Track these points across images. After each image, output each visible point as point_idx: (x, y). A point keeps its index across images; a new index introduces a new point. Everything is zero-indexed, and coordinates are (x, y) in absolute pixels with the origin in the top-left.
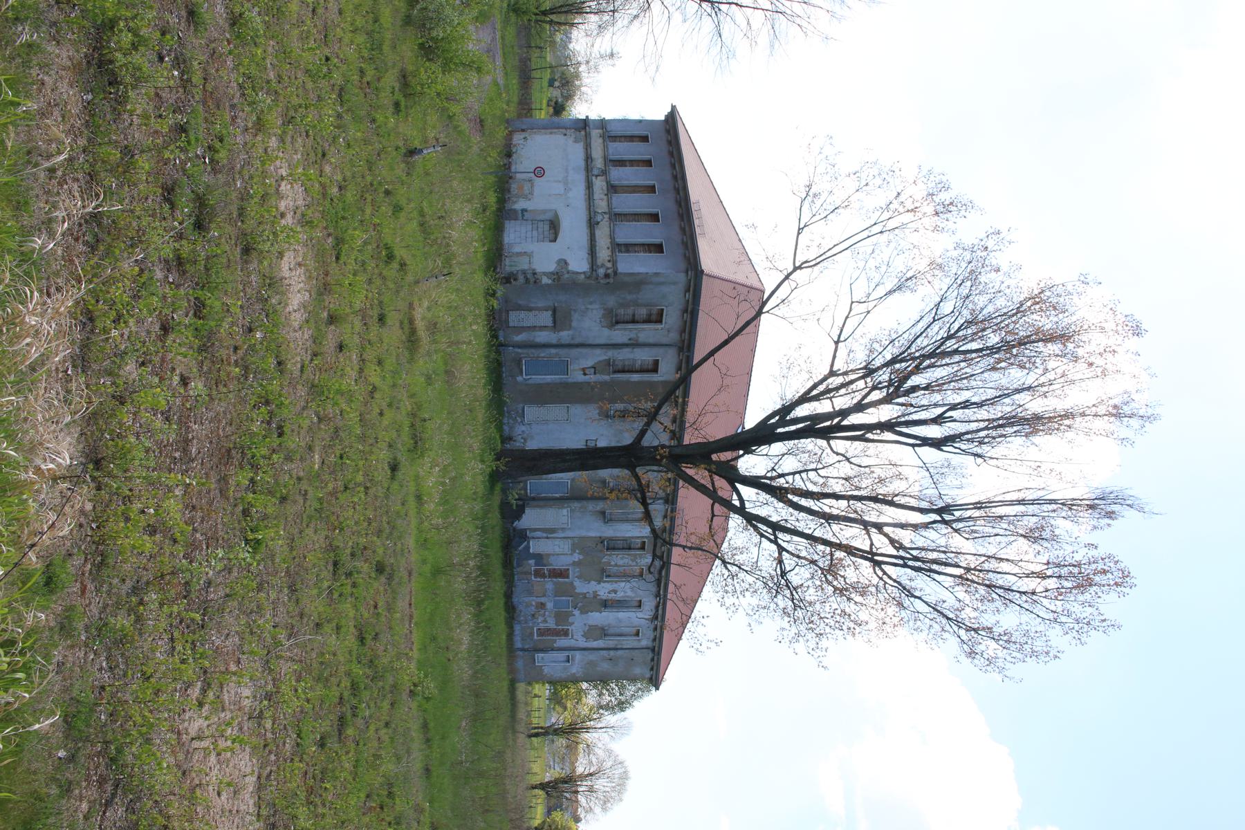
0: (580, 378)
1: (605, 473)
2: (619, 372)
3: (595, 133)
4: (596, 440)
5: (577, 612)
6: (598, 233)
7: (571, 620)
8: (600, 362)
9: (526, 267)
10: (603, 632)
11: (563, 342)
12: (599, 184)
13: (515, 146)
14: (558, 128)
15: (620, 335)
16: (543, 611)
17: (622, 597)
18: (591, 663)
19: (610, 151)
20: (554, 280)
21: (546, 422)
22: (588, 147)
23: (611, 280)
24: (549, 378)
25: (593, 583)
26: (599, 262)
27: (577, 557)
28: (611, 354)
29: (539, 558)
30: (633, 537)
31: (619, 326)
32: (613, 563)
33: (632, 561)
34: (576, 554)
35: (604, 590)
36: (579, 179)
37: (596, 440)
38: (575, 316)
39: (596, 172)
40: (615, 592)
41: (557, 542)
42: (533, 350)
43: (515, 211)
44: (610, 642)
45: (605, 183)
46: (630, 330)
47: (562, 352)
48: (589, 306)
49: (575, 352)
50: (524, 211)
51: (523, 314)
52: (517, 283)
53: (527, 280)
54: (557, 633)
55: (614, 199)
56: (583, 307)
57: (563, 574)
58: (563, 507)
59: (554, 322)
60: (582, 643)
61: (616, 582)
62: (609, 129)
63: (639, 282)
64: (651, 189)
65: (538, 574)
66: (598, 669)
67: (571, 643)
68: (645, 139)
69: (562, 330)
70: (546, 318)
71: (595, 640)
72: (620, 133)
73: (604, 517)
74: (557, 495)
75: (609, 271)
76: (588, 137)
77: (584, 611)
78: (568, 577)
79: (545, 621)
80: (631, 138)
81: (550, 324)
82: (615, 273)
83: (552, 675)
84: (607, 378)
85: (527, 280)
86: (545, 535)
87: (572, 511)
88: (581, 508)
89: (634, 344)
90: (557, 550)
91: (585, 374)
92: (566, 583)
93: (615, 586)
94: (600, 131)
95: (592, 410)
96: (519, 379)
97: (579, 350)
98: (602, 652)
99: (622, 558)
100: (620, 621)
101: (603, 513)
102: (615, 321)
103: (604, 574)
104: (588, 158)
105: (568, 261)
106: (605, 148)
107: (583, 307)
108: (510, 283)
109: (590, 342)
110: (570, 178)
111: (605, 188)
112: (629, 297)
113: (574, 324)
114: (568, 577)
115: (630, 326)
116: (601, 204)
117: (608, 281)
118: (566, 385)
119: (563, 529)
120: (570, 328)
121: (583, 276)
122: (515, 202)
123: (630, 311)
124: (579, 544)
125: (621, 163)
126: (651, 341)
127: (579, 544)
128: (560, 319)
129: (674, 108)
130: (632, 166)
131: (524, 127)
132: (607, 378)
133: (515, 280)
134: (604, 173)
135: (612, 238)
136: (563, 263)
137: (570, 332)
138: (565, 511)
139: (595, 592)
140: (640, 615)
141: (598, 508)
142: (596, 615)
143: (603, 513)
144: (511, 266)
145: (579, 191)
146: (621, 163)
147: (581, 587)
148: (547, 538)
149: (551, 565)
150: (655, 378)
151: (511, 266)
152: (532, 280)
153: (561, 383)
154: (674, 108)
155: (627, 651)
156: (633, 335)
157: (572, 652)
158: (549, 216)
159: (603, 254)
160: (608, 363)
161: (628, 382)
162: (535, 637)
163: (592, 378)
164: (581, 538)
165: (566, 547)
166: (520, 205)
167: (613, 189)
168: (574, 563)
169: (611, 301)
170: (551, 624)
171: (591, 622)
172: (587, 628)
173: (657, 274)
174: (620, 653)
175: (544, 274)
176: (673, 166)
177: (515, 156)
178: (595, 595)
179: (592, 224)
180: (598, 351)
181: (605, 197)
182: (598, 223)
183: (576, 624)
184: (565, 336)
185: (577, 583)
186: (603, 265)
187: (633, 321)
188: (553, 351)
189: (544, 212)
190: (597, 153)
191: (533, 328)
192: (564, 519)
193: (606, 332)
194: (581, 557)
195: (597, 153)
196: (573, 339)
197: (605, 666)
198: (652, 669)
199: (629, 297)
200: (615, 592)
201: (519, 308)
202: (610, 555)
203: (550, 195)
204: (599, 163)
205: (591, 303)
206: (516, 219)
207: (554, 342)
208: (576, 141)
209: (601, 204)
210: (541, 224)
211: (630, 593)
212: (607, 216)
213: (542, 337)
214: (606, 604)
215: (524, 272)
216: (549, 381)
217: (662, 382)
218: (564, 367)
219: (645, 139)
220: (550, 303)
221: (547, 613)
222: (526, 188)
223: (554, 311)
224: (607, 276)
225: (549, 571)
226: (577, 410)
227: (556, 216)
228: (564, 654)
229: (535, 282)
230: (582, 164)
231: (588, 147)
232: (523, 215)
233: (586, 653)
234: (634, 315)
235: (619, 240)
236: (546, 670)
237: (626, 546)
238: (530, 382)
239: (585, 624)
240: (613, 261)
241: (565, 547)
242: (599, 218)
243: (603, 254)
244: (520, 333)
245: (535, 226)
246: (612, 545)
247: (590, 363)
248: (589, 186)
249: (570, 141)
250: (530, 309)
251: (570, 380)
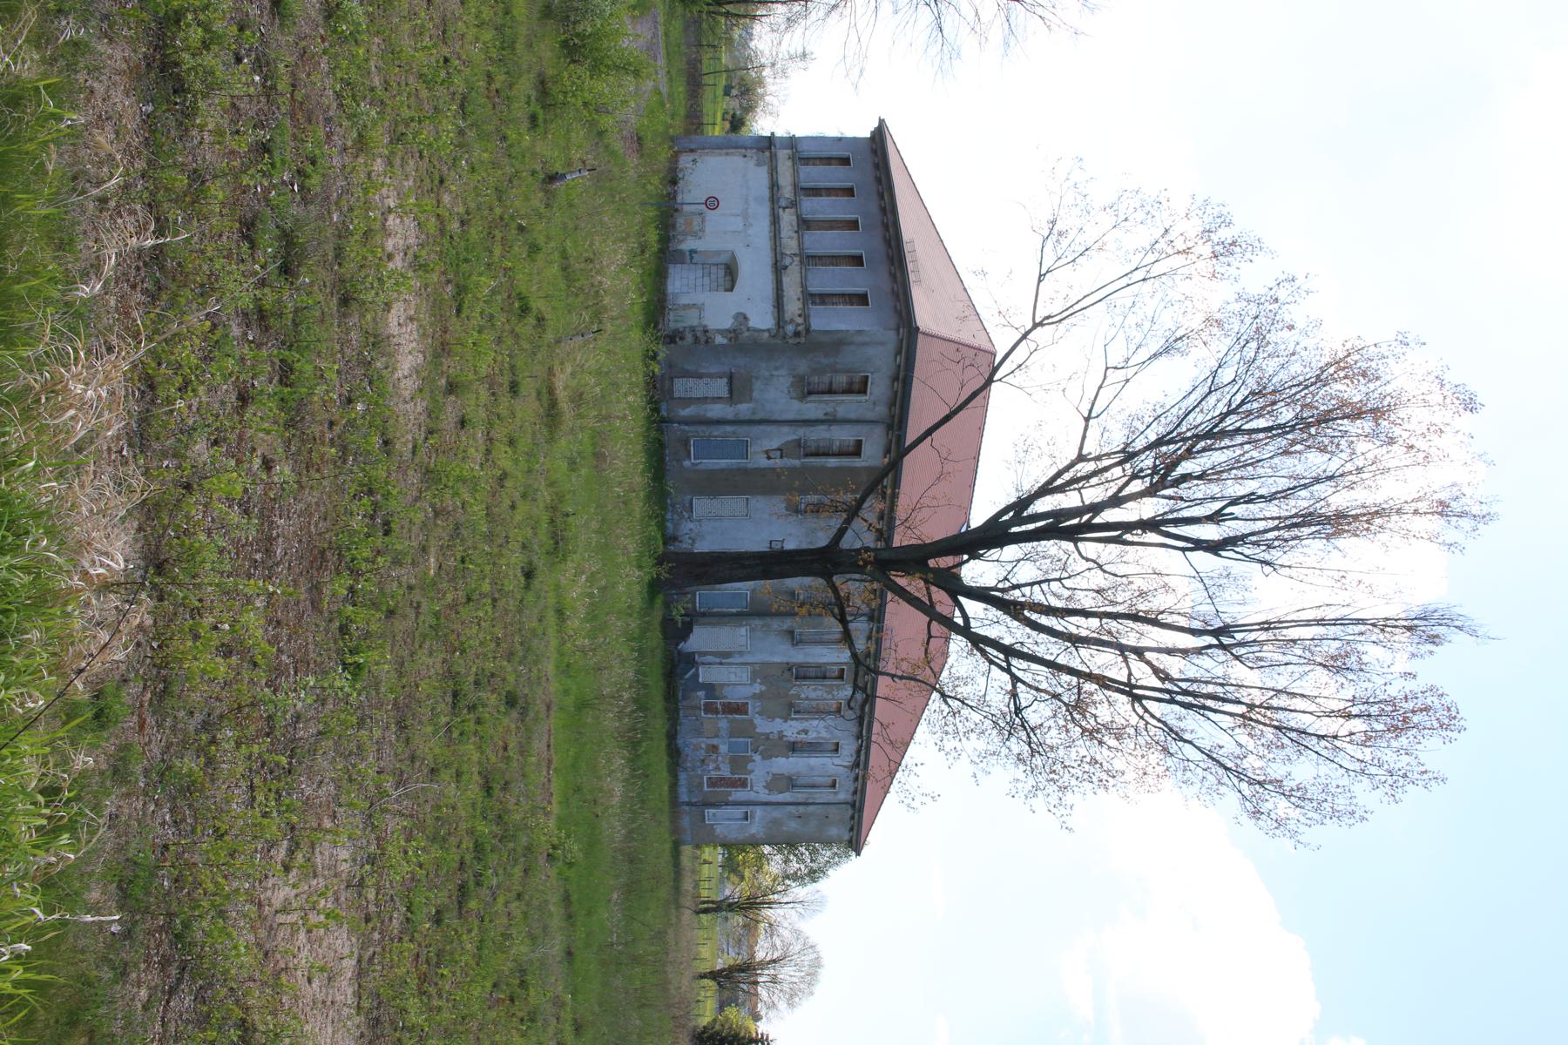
0: (763, 462)
1: (794, 583)
2: (812, 455)
3: (783, 154)
4: (783, 541)
5: (757, 757)
6: (786, 280)
7: (750, 766)
8: (788, 442)
9: (695, 322)
10: (791, 783)
11: (742, 417)
12: (788, 218)
13: (681, 170)
14: (736, 148)
15: (814, 408)
16: (714, 756)
18: (776, 822)
19: (802, 176)
20: (730, 340)
21: (720, 518)
22: (773, 171)
23: (803, 340)
24: (723, 463)
25: (778, 720)
26: (787, 316)
27: (757, 688)
28: (801, 432)
29: (710, 689)
30: (828, 664)
31: (812, 398)
32: (803, 696)
33: (828, 693)
34: (756, 685)
35: (791, 729)
36: (763, 211)
37: (783, 541)
38: (757, 385)
39: (783, 203)
40: (806, 732)
41: (733, 669)
42: (704, 428)
43: (681, 252)
44: (800, 795)
45: (794, 218)
46: (826, 402)
47: (741, 430)
48: (776, 373)
49: (756, 430)
50: (692, 252)
51: (691, 382)
52: (685, 343)
53: (696, 339)
55: (806, 237)
56: (767, 374)
57: (740, 709)
58: (741, 625)
59: (731, 391)
60: (764, 796)
61: (807, 720)
62: (800, 149)
63: (837, 343)
64: (853, 225)
65: (710, 708)
67: (752, 796)
68: (845, 161)
69: (741, 402)
70: (720, 387)
72: (813, 154)
73: (793, 638)
74: (734, 610)
75: (800, 328)
76: (773, 158)
77: (767, 756)
78: (746, 713)
79: (718, 768)
80: (828, 161)
81: (724, 393)
82: (808, 330)
84: (796, 462)
85: (696, 339)
86: (718, 660)
87: (752, 630)
88: (763, 626)
89: (831, 421)
90: (733, 678)
91: (769, 458)
92: (743, 720)
93: (805, 725)
94: (789, 151)
95: (778, 503)
96: (686, 463)
97: (762, 427)
99: (815, 690)
101: (791, 633)
102: (806, 390)
103: (791, 710)
104: (774, 186)
105: (749, 315)
106: (795, 172)
107: (767, 374)
108: (675, 342)
109: (776, 417)
110: (750, 211)
111: (795, 223)
112: (825, 361)
113: (755, 394)
114: (746, 713)
115: (826, 397)
116: (790, 244)
117: (798, 340)
118: (744, 471)
119: (741, 653)
120: (751, 400)
121: (766, 334)
122: (681, 242)
123: (826, 379)
124: (761, 672)
125: (815, 192)
126: (853, 416)
127: (761, 672)
128: (737, 389)
129: (882, 122)
130: (829, 195)
131: (693, 146)
132: (796, 462)
133: (682, 338)
134: (794, 204)
135: (804, 286)
136: (742, 318)
137: (751, 405)
138: (743, 631)
139: (780, 732)
140: (837, 761)
141: (785, 627)
142: (782, 760)
143: (791, 633)
144: (676, 321)
145: (762, 228)
146: (815, 192)
147: (763, 726)
148: (721, 664)
149: (726, 697)
150: (857, 462)
151: (676, 321)
152: (703, 339)
153: (739, 469)
154: (882, 122)
156: (829, 409)
158: (724, 259)
159: (793, 307)
160: (798, 443)
161: (824, 469)
162: (706, 788)
163: (778, 463)
165: (745, 675)
166: (688, 244)
167: (805, 224)
168: (754, 696)
169: (803, 366)
170: (725, 772)
171: (775, 770)
173: (860, 332)
174: (811, 808)
175: (719, 331)
176: (881, 196)
177: (681, 184)
178: (781, 735)
179: (778, 269)
180: (785, 429)
181: (795, 235)
182: (786, 268)
184: (744, 409)
185: (758, 721)
186: (792, 321)
187: (830, 391)
188: (729, 428)
189: (718, 253)
190: (785, 179)
191: (704, 400)
192: (742, 641)
193: (796, 405)
194: (764, 688)
195: (785, 179)
196: (754, 413)
197: (792, 826)
198: (851, 829)
199: (825, 361)
200: (806, 732)
201: (687, 374)
202: (799, 686)
203: (725, 233)
204: (787, 192)
205: (776, 369)
206: (683, 262)
207: (730, 417)
208: (759, 164)
209: (790, 244)
210: (714, 269)
211: (824, 734)
212: (797, 259)
213: (716, 411)
214: (794, 748)
215: (693, 329)
216: (724, 466)
217: (866, 468)
218: (742, 449)
219: (845, 161)
220: (726, 369)
222: (695, 223)
223: (731, 378)
224: (797, 334)
225: (723, 705)
226: (760, 504)
227: (733, 258)
228: (744, 809)
229: (707, 342)
230: (766, 193)
231: (773, 171)
232: (692, 258)
233: (769, 808)
234: (831, 383)
235: (812, 289)
236: (718, 830)
237: (820, 674)
238: (700, 467)
240: (805, 316)
241: (744, 675)
242: (787, 261)
243: (793, 307)
244: (688, 406)
245: (706, 271)
246: (802, 673)
247: (775, 444)
248: (775, 221)
249: (752, 163)
250: (700, 376)
251: (749, 466)
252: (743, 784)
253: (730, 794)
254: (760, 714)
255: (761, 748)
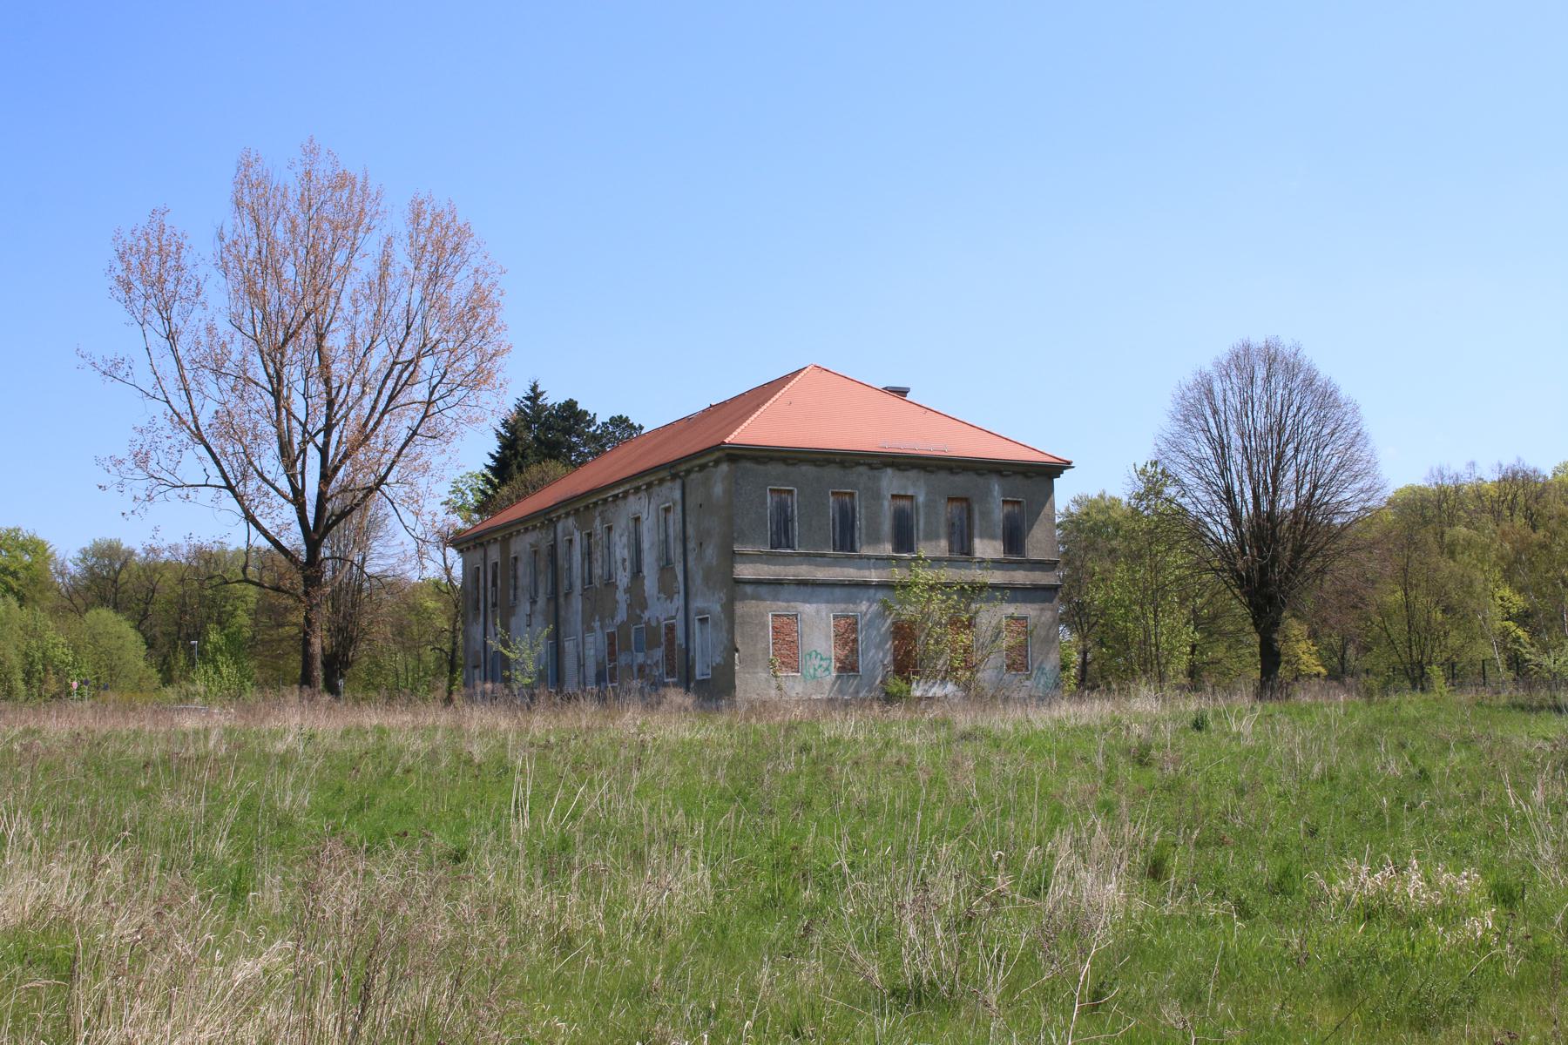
5: (646, 615)
7: (654, 624)
10: (666, 567)
17: (629, 551)
35: (623, 578)
41: (587, 652)
44: (676, 551)
54: (671, 641)
60: (679, 601)
66: (715, 563)
67: (680, 616)
71: (676, 577)
83: (725, 649)
90: (592, 652)
98: (691, 558)
100: (652, 544)
103: (610, 584)
114: (613, 633)
147: (622, 615)
149: (604, 657)
155: (688, 519)
157: (692, 615)
164: (583, 623)
170: (659, 654)
172: (662, 595)
174: (690, 531)
183: (658, 615)
197: (711, 552)
198: (702, 467)
214: (637, 572)
221: (649, 662)
225: (610, 661)
228: (696, 626)
233: (693, 590)
236: (718, 660)
239: (658, 599)
241: (590, 639)
252: (671, 629)
253: (680, 645)
254: (613, 619)
255: (638, 612)
